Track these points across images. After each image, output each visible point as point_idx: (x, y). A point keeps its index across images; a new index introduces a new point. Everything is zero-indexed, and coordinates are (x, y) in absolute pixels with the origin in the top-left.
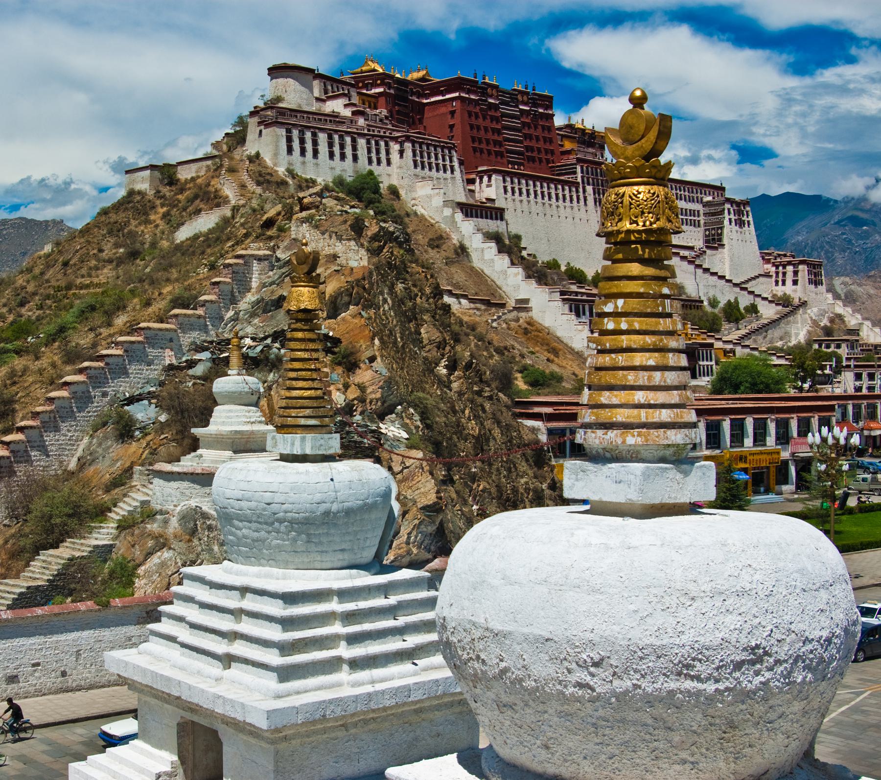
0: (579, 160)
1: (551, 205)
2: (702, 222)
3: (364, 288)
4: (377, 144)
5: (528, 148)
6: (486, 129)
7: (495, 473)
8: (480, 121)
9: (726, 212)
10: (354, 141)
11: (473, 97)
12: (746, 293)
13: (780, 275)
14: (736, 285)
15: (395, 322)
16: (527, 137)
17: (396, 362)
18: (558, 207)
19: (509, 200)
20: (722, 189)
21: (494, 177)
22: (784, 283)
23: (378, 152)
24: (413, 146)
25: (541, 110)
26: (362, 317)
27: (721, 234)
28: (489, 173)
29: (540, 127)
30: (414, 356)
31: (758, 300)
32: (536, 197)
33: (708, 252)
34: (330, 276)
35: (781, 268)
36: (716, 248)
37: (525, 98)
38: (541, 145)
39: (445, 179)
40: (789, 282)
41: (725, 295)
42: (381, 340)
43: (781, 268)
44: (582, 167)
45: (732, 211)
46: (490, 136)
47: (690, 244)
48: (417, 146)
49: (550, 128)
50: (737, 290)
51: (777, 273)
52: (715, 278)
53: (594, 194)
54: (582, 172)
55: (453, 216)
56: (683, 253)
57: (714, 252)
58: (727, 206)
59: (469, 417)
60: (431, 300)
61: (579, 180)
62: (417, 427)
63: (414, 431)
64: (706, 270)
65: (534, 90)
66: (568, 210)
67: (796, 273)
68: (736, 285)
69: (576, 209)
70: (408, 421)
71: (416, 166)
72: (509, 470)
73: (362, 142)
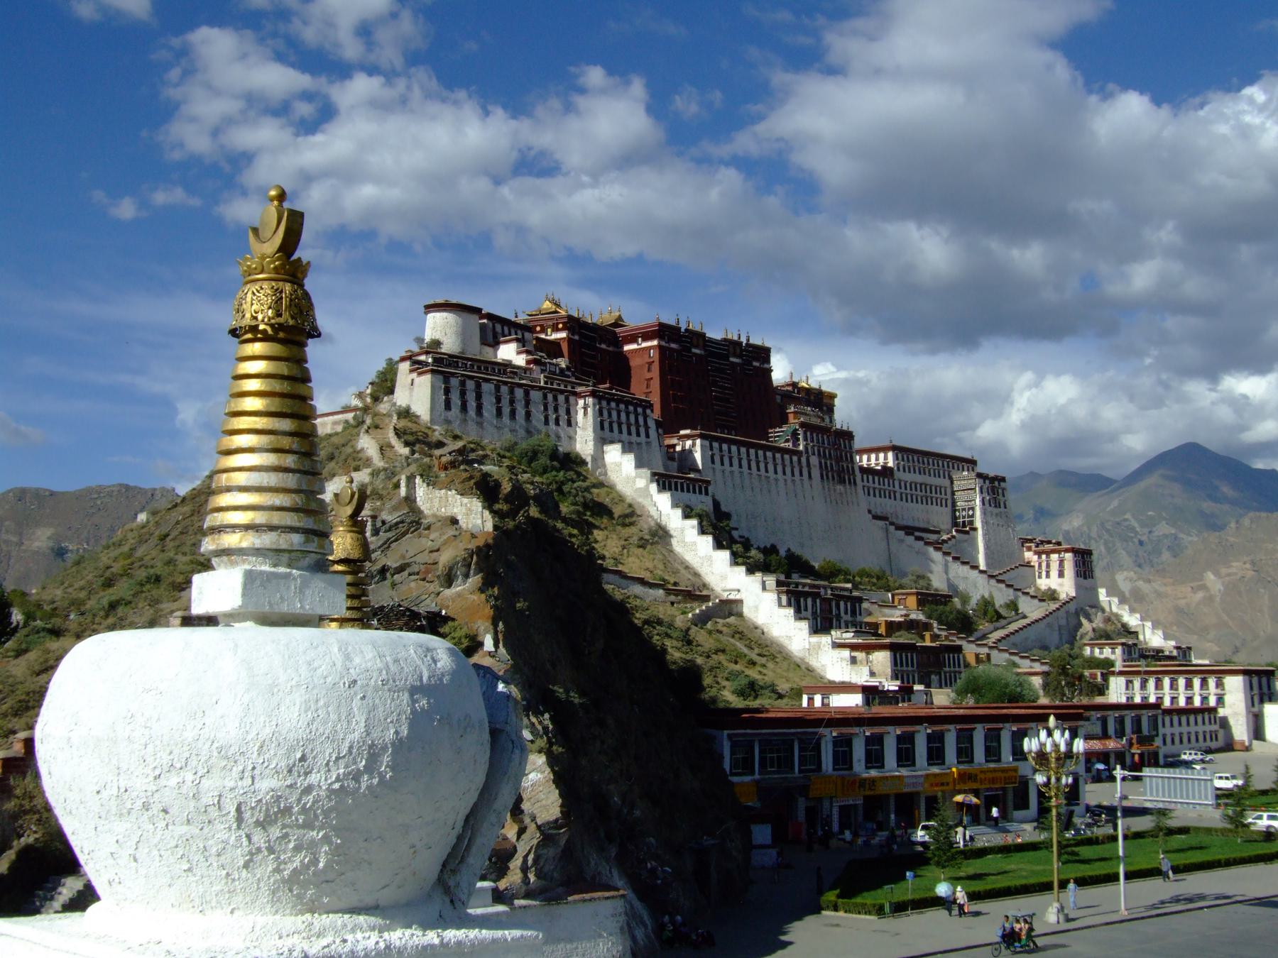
0: (803, 425)
4: (555, 399)
10: (527, 394)
11: (673, 346)
12: (1003, 586)
13: (1044, 565)
20: (972, 463)
22: (1048, 576)
23: (556, 410)
25: (756, 364)
27: (972, 516)
34: (445, 543)
35: (1044, 557)
36: (967, 533)
37: (738, 351)
39: (639, 444)
40: (1054, 573)
43: (1044, 557)
44: (805, 433)
45: (985, 490)
48: (604, 403)
50: (993, 582)
52: (966, 568)
54: (806, 439)
55: (647, 486)
62: (545, 728)
67: (1061, 562)
68: (991, 577)
71: (602, 428)
73: (536, 395)
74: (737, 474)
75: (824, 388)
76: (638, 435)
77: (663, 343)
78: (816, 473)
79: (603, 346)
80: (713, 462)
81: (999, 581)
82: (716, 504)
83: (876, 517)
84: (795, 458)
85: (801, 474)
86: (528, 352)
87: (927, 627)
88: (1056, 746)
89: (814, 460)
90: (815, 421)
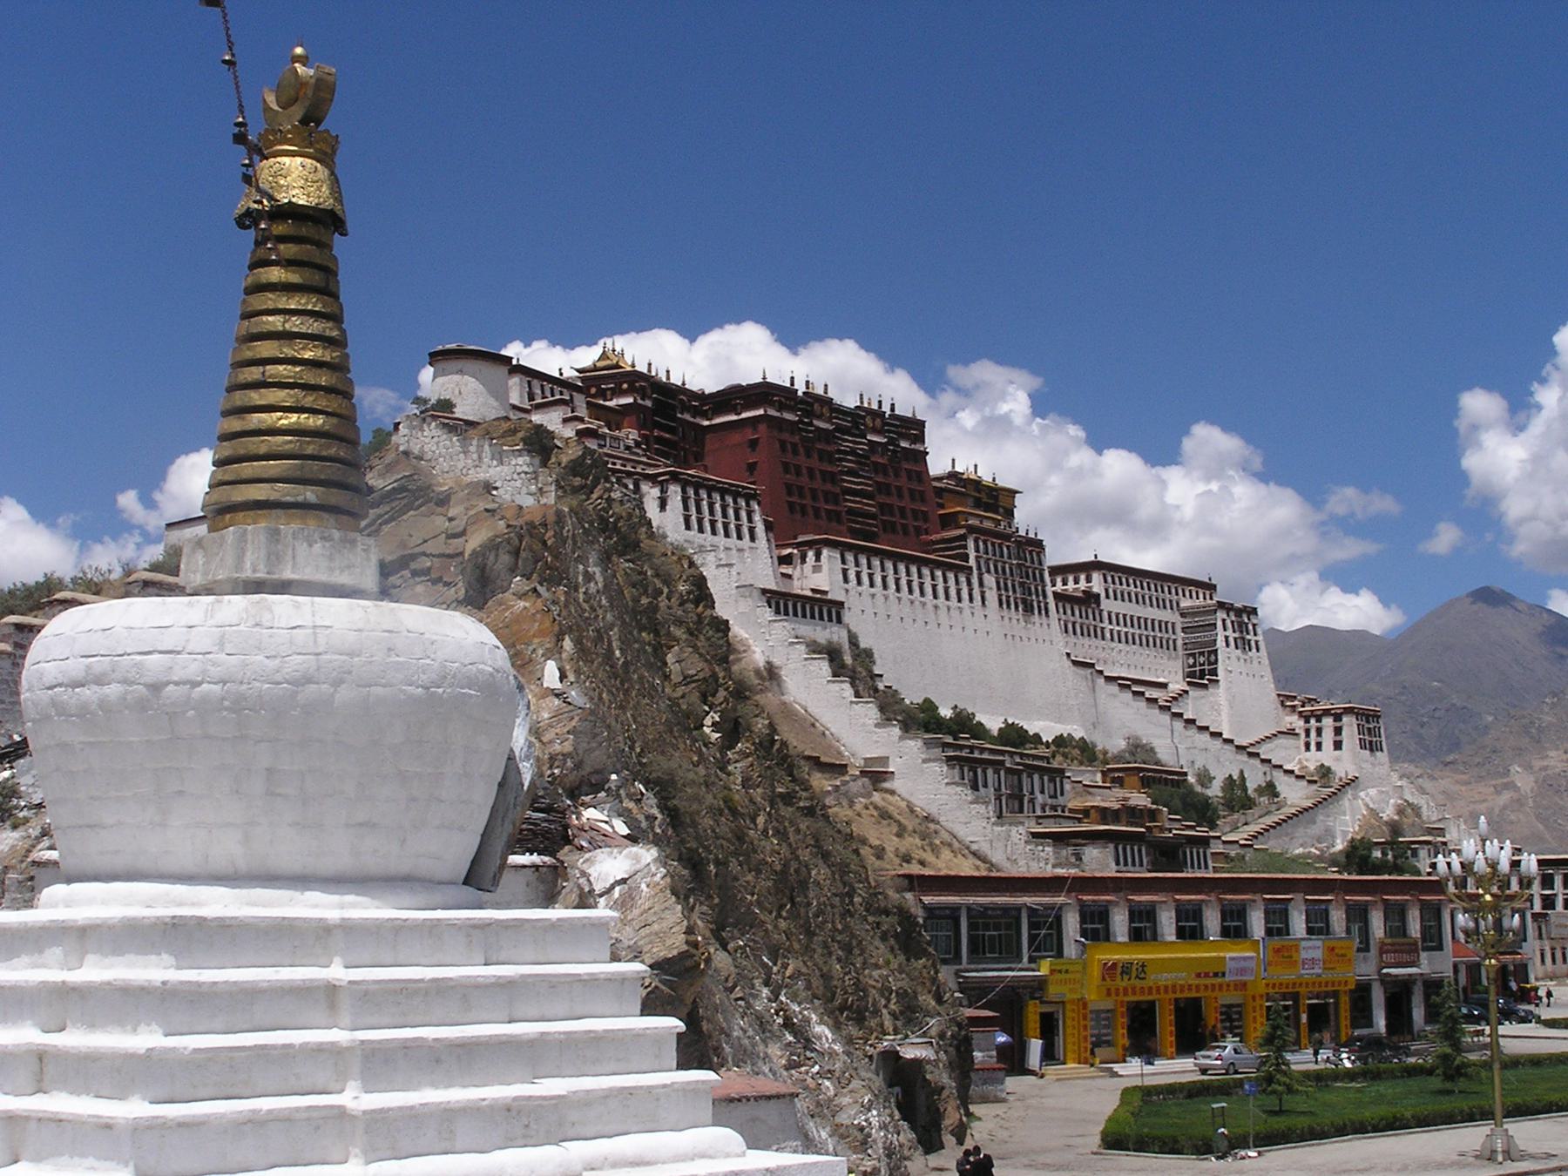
0: (971, 529)
1: (924, 604)
2: (1180, 643)
3: (544, 543)
5: (882, 506)
6: (811, 471)
7: (819, 951)
8: (802, 460)
9: (1219, 623)
11: (789, 416)
12: (1256, 762)
13: (1313, 734)
14: (1240, 748)
15: (609, 617)
16: (883, 488)
17: (610, 692)
18: (936, 607)
19: (852, 593)
20: (1210, 587)
21: (825, 552)
22: (1319, 746)
24: (684, 491)
25: (904, 444)
26: (539, 595)
28: (817, 546)
29: (903, 474)
30: (651, 693)
31: (1278, 774)
32: (898, 590)
33: (1193, 693)
35: (1313, 721)
36: (1205, 686)
37: (878, 422)
38: (906, 502)
41: (1225, 765)
42: (578, 642)
43: (1313, 721)
44: (976, 541)
46: (818, 484)
47: (1161, 680)
48: (691, 492)
49: (921, 473)
51: (1308, 732)
52: (1206, 737)
53: (999, 588)
54: (977, 550)
56: (1151, 693)
57: (1201, 692)
58: (1221, 615)
59: (765, 831)
60: (690, 606)
61: (972, 562)
62: (651, 818)
63: (644, 825)
64: (1191, 722)
65: (893, 409)
66: (954, 613)
67: (1338, 731)
69: (967, 612)
70: (631, 805)
71: (688, 527)
72: (848, 949)
74: (880, 599)
75: (1001, 483)
76: (740, 537)
77: (772, 412)
78: (992, 596)
79: (687, 417)
80: (846, 580)
81: (1251, 755)
82: (853, 640)
83: (1075, 663)
84: (963, 579)
85: (971, 600)
86: (581, 420)
87: (1153, 815)
88: (1493, 865)
89: (990, 580)
90: (988, 524)
